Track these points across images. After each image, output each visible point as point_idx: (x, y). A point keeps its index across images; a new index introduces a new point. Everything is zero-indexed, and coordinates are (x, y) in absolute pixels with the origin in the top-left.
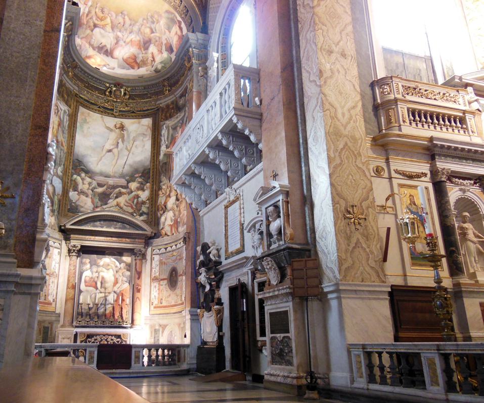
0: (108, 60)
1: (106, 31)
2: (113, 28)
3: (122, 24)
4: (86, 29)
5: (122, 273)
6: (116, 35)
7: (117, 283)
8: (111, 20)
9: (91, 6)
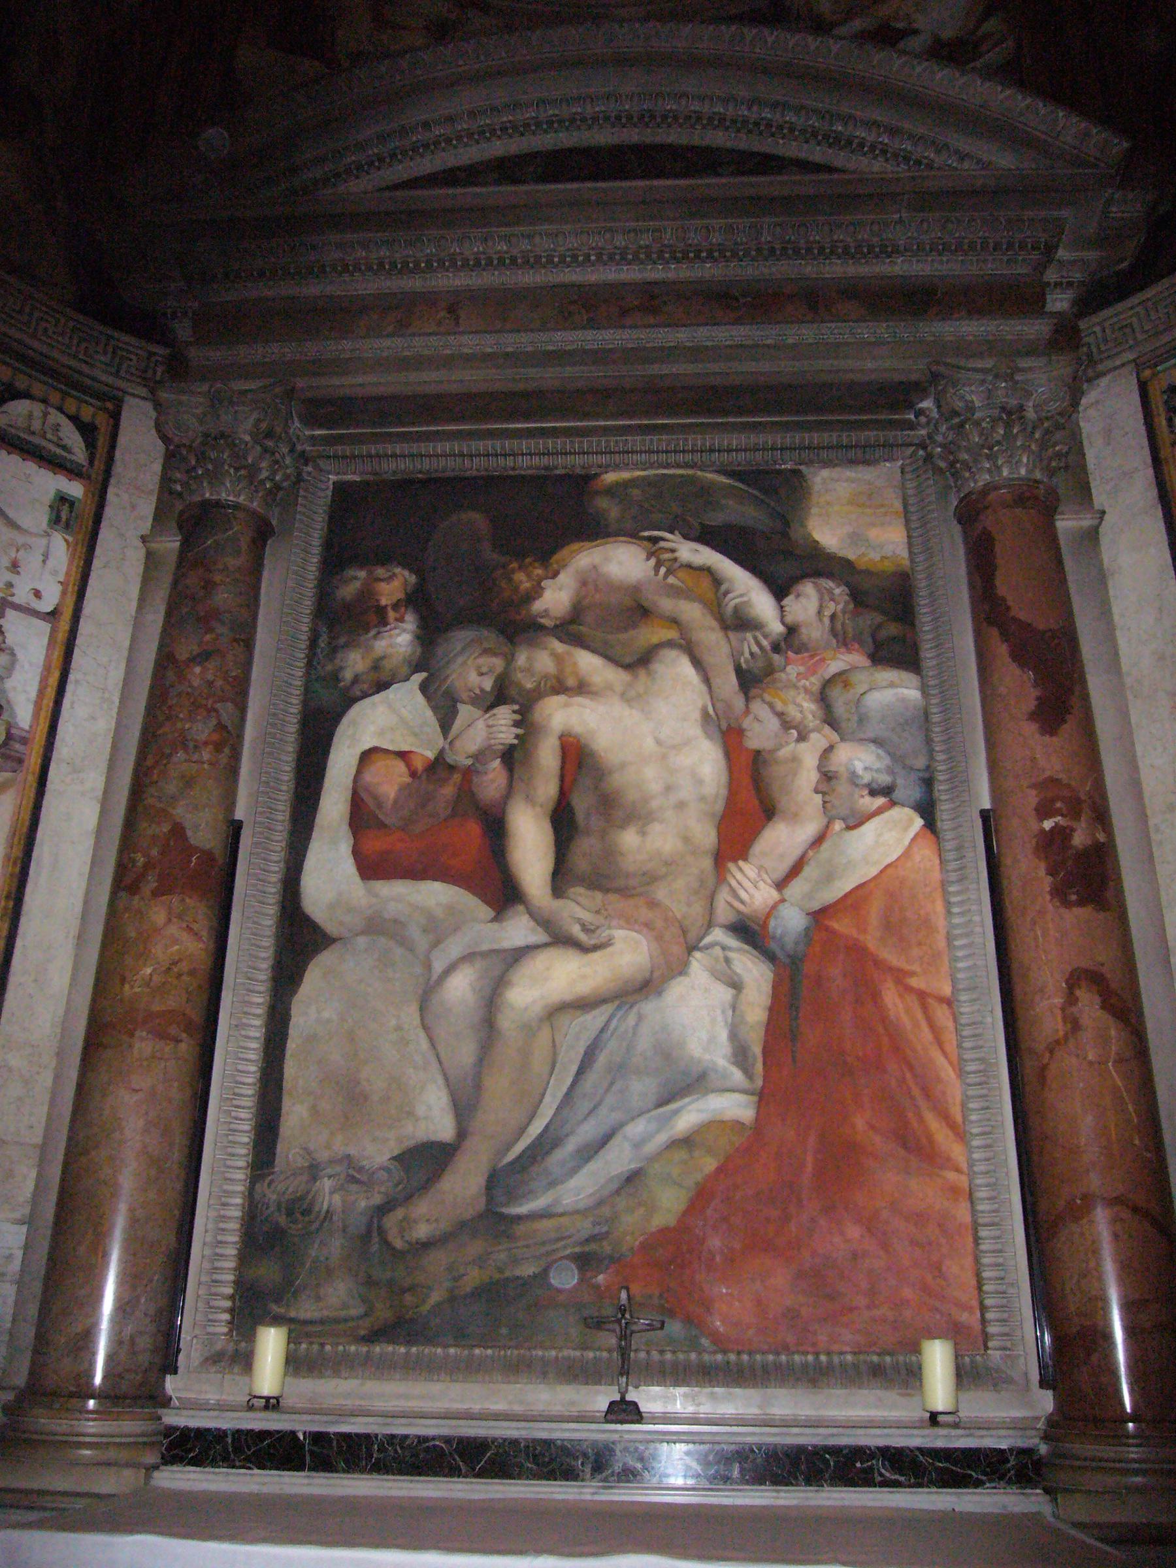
5: (823, 698)
7: (769, 812)
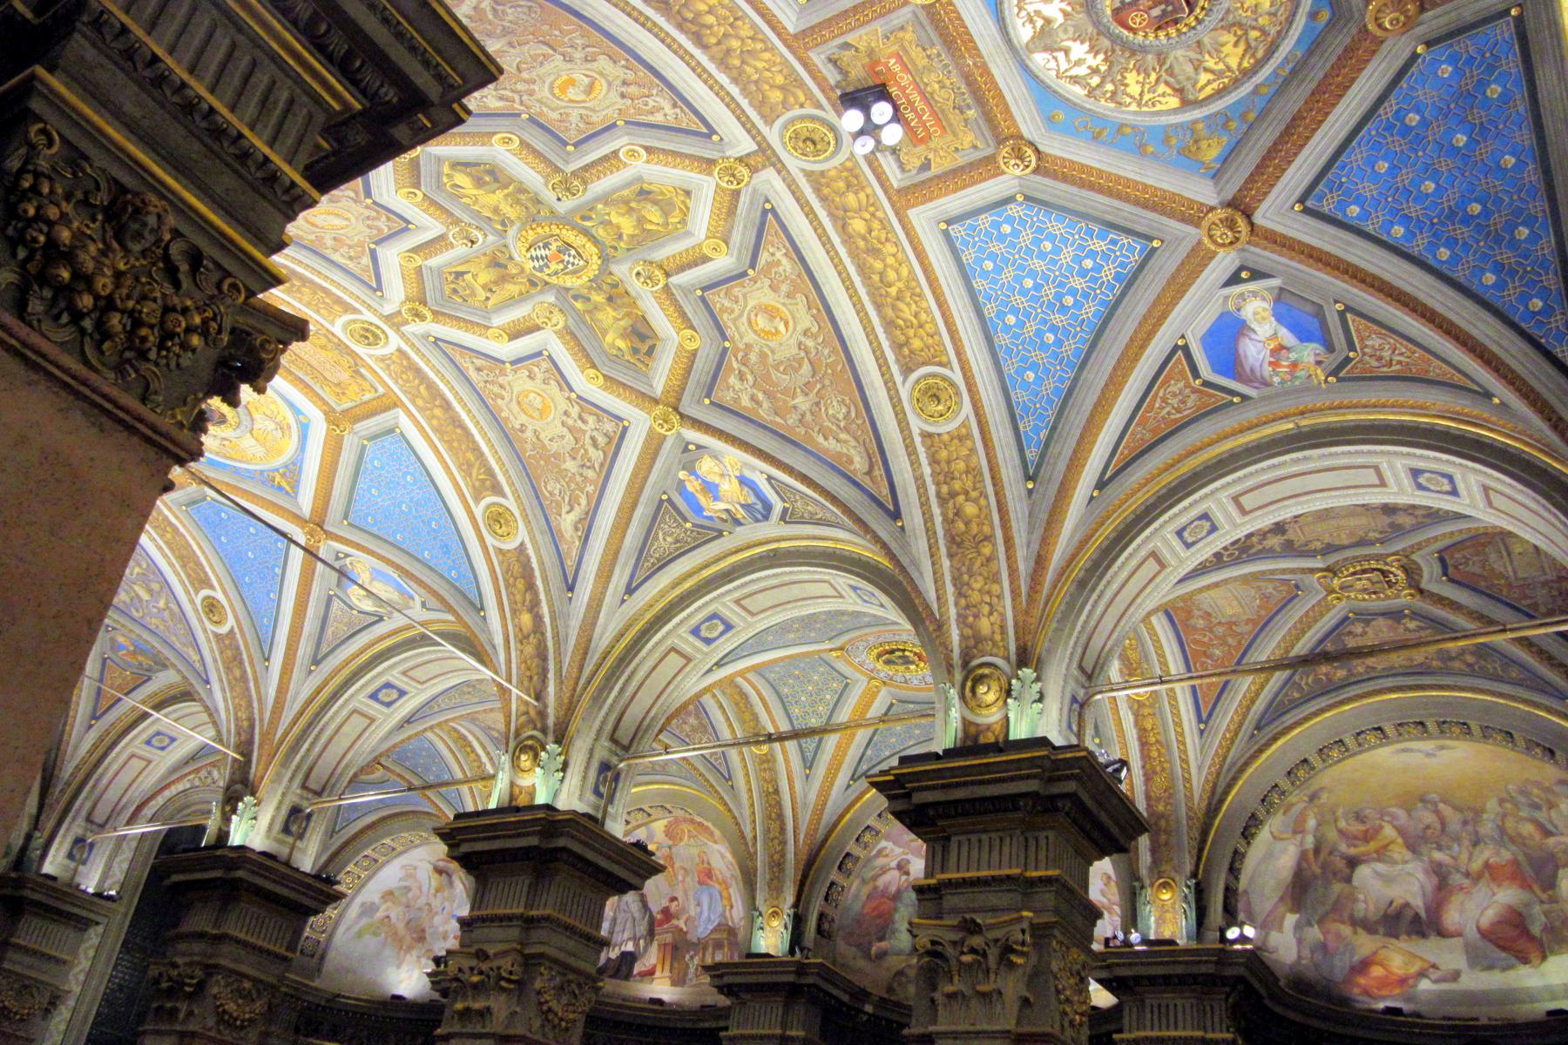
0: (1430, 949)
1: (1395, 863)
2: (1412, 847)
3: (1438, 826)
4: (1327, 884)
6: (1431, 861)
8: (1395, 827)
9: (1319, 825)
